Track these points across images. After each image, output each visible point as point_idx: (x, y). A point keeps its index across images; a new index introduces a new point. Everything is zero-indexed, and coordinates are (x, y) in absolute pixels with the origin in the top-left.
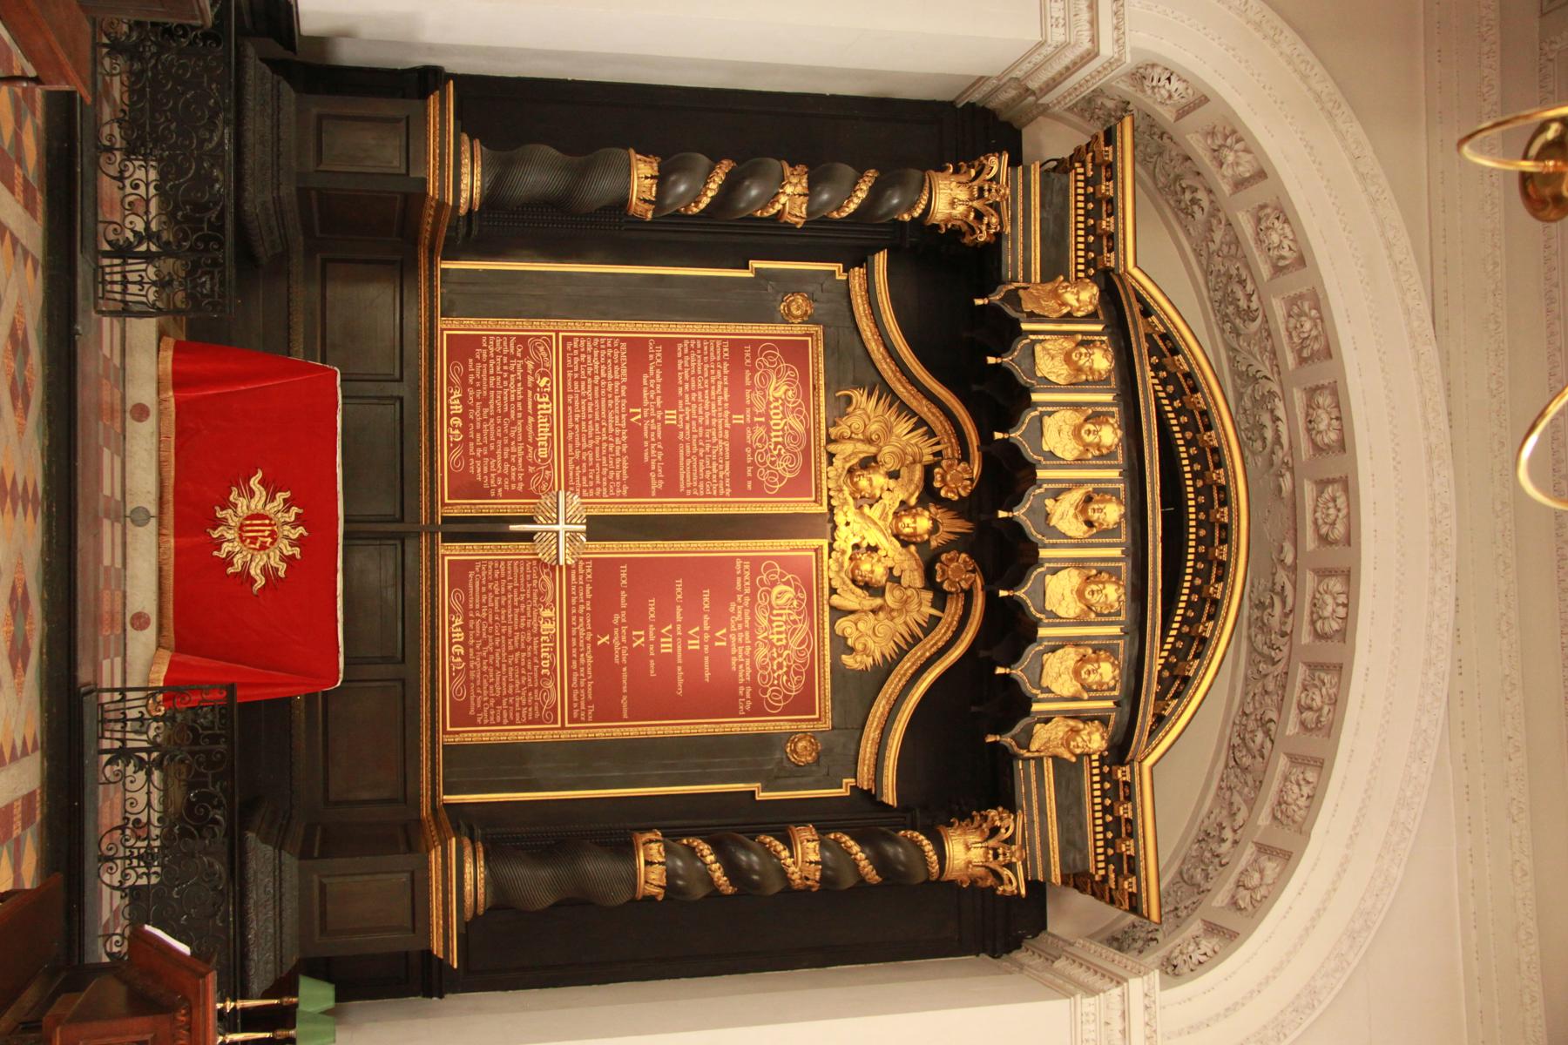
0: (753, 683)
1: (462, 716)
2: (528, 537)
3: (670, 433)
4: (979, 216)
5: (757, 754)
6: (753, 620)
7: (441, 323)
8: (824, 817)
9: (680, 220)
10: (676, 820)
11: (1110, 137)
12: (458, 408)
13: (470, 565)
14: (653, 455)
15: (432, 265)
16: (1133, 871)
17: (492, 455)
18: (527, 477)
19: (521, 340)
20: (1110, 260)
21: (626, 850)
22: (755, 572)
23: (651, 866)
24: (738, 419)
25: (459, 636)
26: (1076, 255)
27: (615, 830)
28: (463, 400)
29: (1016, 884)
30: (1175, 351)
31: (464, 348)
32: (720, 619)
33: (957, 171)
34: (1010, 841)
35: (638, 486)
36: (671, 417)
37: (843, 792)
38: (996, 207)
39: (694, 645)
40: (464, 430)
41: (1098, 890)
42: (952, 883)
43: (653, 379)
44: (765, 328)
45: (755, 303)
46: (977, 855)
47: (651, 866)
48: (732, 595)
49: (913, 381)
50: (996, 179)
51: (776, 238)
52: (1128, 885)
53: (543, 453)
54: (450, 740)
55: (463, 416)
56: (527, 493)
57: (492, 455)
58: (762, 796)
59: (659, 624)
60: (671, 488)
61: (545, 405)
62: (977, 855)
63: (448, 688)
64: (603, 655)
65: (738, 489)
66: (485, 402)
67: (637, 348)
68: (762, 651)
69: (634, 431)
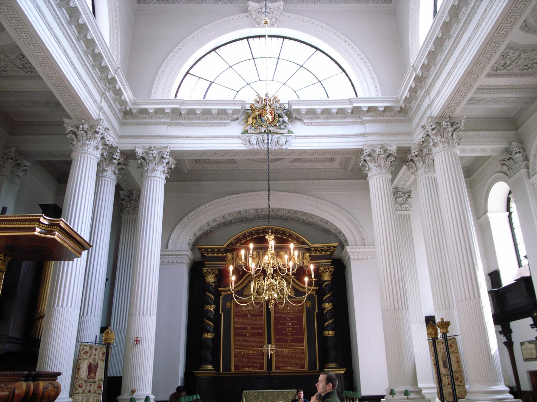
0: (297, 313)
1: (303, 367)
2: (271, 355)
3: (252, 328)
4: (214, 273)
5: (310, 312)
6: (286, 313)
7: (232, 372)
8: (321, 302)
9: (214, 328)
10: (322, 329)
11: (201, 249)
12: (248, 368)
13: (276, 366)
14: (256, 332)
15: (222, 374)
16: (330, 247)
17: (256, 362)
18: (260, 355)
19: (235, 357)
20: (222, 250)
21: (327, 338)
22: (277, 312)
23: (330, 333)
24: (249, 316)
25: (289, 368)
26: (221, 255)
27: (323, 339)
28: (246, 367)
29: (332, 268)
30: (238, 238)
31: (236, 368)
32: (285, 319)
33: (205, 276)
34: (324, 269)
35: (261, 334)
36: (249, 328)
37: (316, 296)
38: (212, 270)
39: (290, 324)
40: (251, 367)
41: (332, 252)
42: (332, 278)
43: (242, 332)
44: (232, 311)
45: (227, 313)
46: (327, 274)
47: (330, 333)
48: (281, 317)
49: (242, 283)
50: (207, 270)
51: (217, 309)
52: (332, 248)
53: (256, 352)
54: (308, 369)
55: (249, 367)
56: (263, 355)
57: (256, 362)
58: (317, 311)
59: (286, 330)
60: (262, 328)
61: (247, 352)
62: (327, 274)
63: (298, 370)
64: (292, 341)
65: (262, 316)
66: (246, 363)
67: (236, 335)
68: (291, 311)
69: (251, 335)
